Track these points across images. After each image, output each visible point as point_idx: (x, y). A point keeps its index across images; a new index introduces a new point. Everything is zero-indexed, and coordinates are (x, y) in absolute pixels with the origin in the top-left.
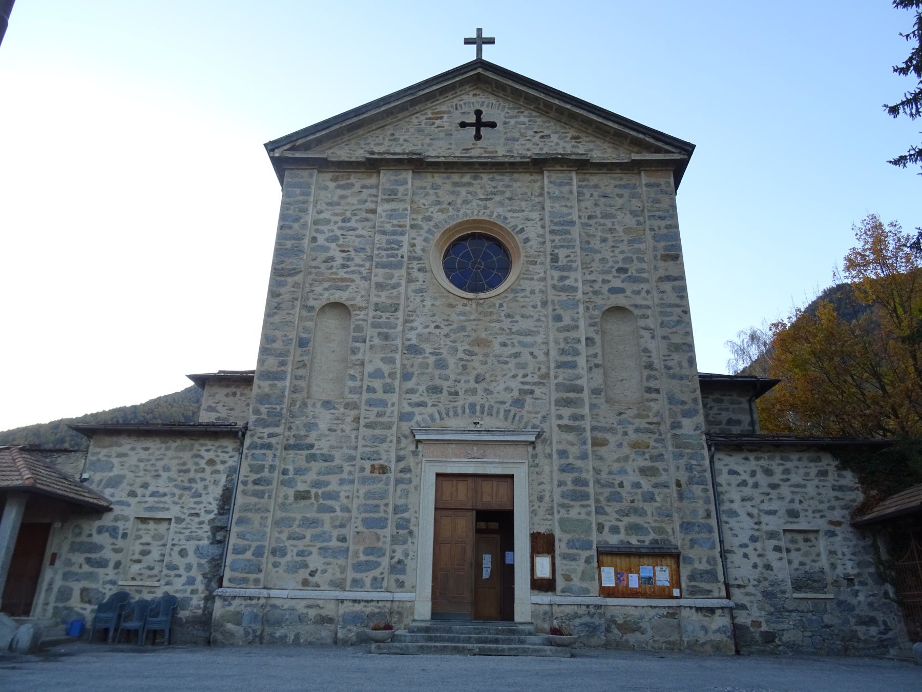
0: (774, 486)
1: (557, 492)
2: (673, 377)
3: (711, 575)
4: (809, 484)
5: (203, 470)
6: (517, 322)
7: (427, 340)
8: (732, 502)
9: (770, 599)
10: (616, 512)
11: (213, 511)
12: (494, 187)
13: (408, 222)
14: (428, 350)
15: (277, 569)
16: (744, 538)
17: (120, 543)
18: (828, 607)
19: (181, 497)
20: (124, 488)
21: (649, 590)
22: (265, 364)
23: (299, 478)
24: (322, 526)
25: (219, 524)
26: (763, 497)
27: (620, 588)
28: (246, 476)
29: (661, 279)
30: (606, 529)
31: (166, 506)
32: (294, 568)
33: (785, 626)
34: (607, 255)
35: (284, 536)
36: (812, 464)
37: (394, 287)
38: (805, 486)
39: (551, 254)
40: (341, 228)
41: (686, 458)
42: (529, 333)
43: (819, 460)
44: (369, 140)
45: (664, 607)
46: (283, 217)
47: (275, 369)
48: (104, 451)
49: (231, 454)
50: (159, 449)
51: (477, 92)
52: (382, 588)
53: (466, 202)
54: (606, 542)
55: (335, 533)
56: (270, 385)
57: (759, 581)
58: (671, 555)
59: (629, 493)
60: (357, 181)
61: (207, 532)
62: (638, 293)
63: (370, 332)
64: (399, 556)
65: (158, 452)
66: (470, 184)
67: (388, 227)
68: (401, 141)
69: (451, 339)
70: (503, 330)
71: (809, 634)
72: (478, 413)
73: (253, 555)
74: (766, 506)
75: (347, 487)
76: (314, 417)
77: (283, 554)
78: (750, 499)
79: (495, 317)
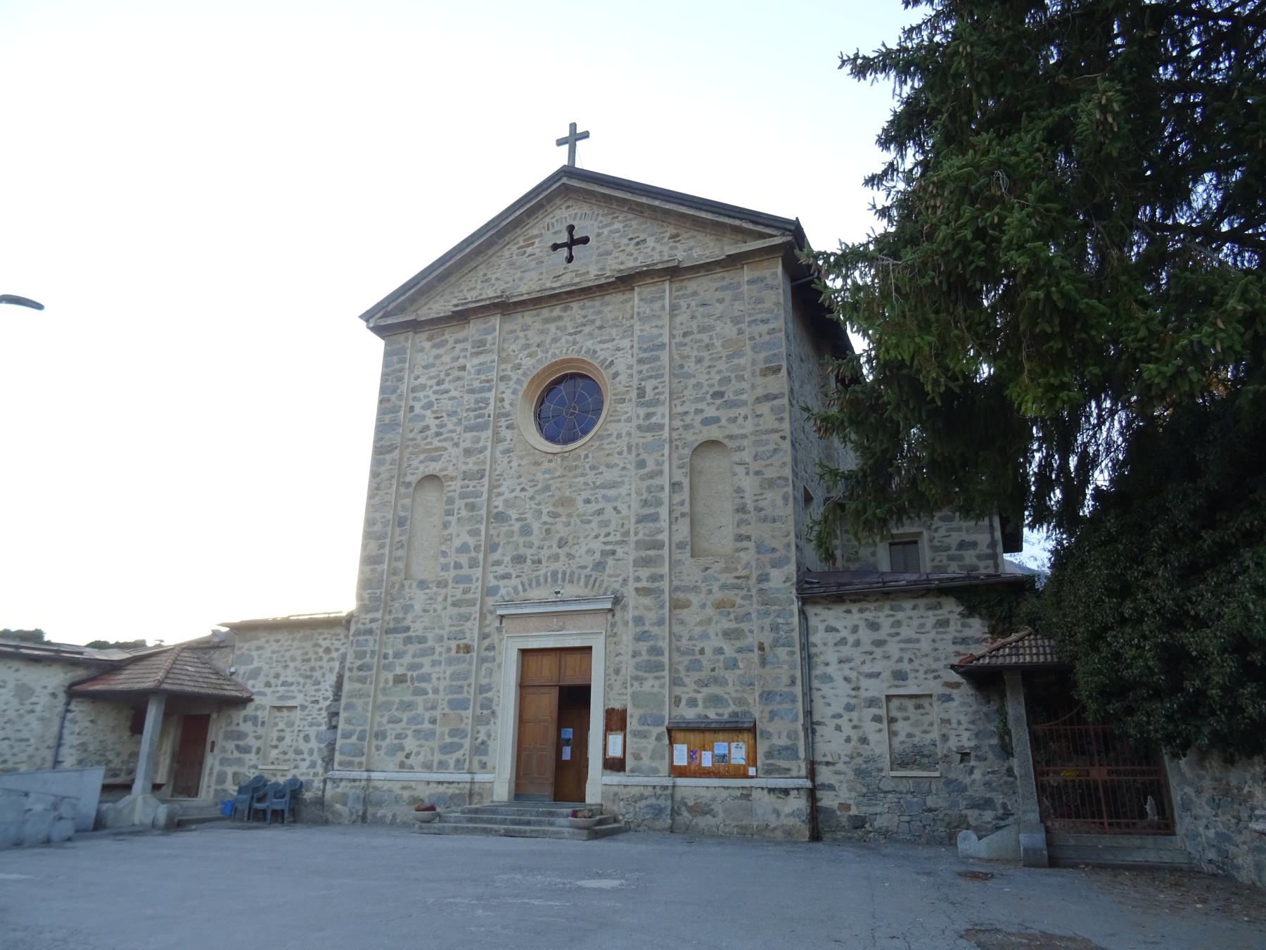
0: (879, 643)
2: (765, 520)
3: (791, 751)
4: (923, 637)
6: (601, 473)
8: (827, 664)
9: (863, 778)
10: (695, 683)
12: (585, 317)
13: (494, 375)
14: (514, 516)
16: (837, 707)
17: (260, 730)
18: (934, 787)
20: (262, 679)
21: (723, 770)
23: (397, 661)
26: (864, 657)
27: (693, 767)
28: (352, 663)
29: (758, 400)
30: (683, 702)
31: (294, 694)
32: (393, 750)
33: (878, 809)
34: (702, 378)
35: (385, 720)
36: (930, 613)
37: (481, 452)
38: (918, 641)
39: (638, 389)
40: (435, 392)
41: (772, 617)
42: (614, 485)
43: (939, 606)
44: (462, 287)
45: (738, 788)
46: (383, 390)
48: (247, 645)
50: (287, 640)
51: (569, 203)
53: (555, 340)
54: (682, 716)
57: (852, 758)
58: (749, 730)
59: (710, 660)
60: (450, 336)
62: (734, 420)
63: (459, 503)
64: (482, 736)
66: (560, 318)
67: (476, 384)
68: (493, 281)
69: (536, 501)
70: (588, 485)
71: (907, 818)
72: (559, 582)
74: (867, 669)
75: (437, 669)
77: (384, 738)
78: (849, 660)
79: (579, 471)
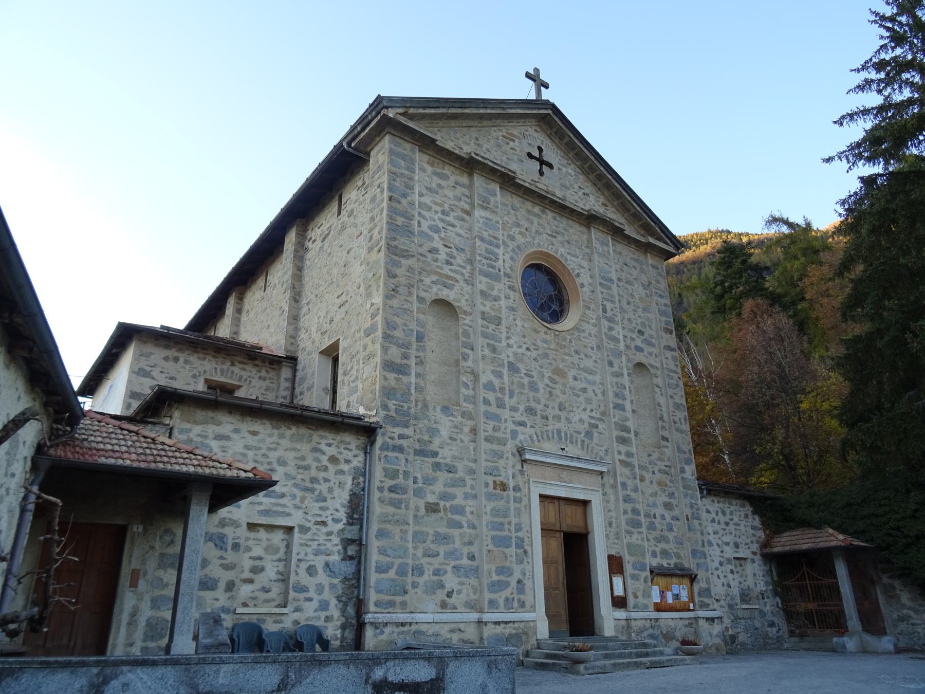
1: (623, 518)
5: (326, 469)
7: (521, 361)
11: (342, 520)
14: (523, 371)
15: (416, 590)
17: (231, 556)
19: (303, 499)
22: (389, 352)
24: (454, 543)
25: (349, 537)
28: (381, 482)
31: (286, 510)
47: (398, 361)
48: (197, 429)
49: (355, 452)
50: (271, 436)
52: (513, 608)
55: (465, 550)
56: (395, 378)
59: (659, 523)
61: (337, 545)
62: (651, 354)
63: (480, 341)
65: (269, 440)
72: (563, 440)
73: (397, 573)
75: (470, 502)
76: (436, 423)
77: (421, 573)
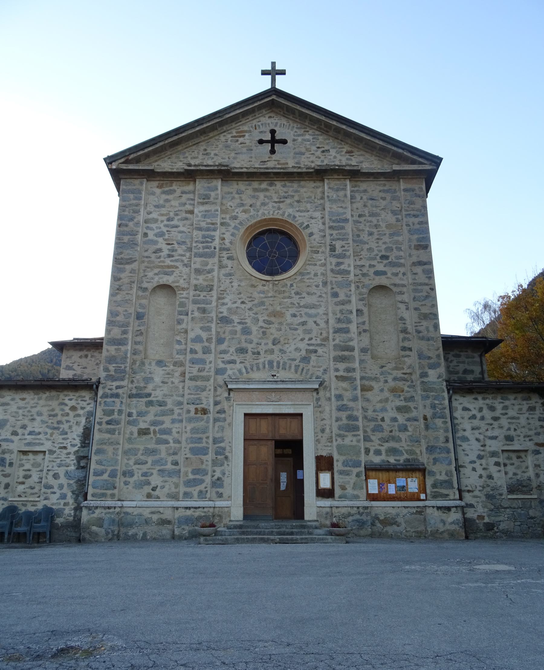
0: (496, 419)
1: (335, 425)
2: (422, 338)
3: (448, 484)
5: (68, 415)
7: (236, 313)
8: (465, 430)
9: (491, 500)
10: (379, 439)
11: (77, 445)
12: (286, 192)
13: (218, 221)
14: (236, 321)
15: (127, 486)
17: (8, 470)
18: (533, 504)
19: (52, 435)
22: (111, 332)
23: (141, 419)
24: (160, 454)
25: (82, 455)
26: (487, 427)
27: (382, 494)
28: (100, 419)
29: (414, 264)
30: (372, 452)
31: (41, 442)
32: (140, 485)
33: (501, 518)
34: (373, 245)
35: (131, 462)
36: (525, 402)
37: (209, 272)
38: (518, 418)
39: (330, 245)
40: (166, 226)
41: (431, 399)
42: (313, 306)
43: (529, 399)
44: (187, 155)
45: (414, 507)
46: (120, 217)
47: (119, 337)
49: (88, 402)
50: (33, 399)
51: (272, 115)
52: (206, 498)
53: (263, 204)
54: (371, 461)
55: (170, 459)
56: (115, 349)
57: (483, 487)
58: (419, 470)
59: (388, 425)
60: (178, 187)
61: (73, 460)
62: (396, 274)
63: (191, 307)
64: (218, 474)
65: (32, 402)
66: (267, 190)
67: (203, 225)
68: (212, 155)
69: (254, 312)
70: (294, 304)
71: (519, 523)
72: (275, 368)
73: (109, 476)
74: (489, 434)
75: (177, 425)
76: (150, 373)
77: (132, 475)
78: (478, 428)
79: (287, 294)
